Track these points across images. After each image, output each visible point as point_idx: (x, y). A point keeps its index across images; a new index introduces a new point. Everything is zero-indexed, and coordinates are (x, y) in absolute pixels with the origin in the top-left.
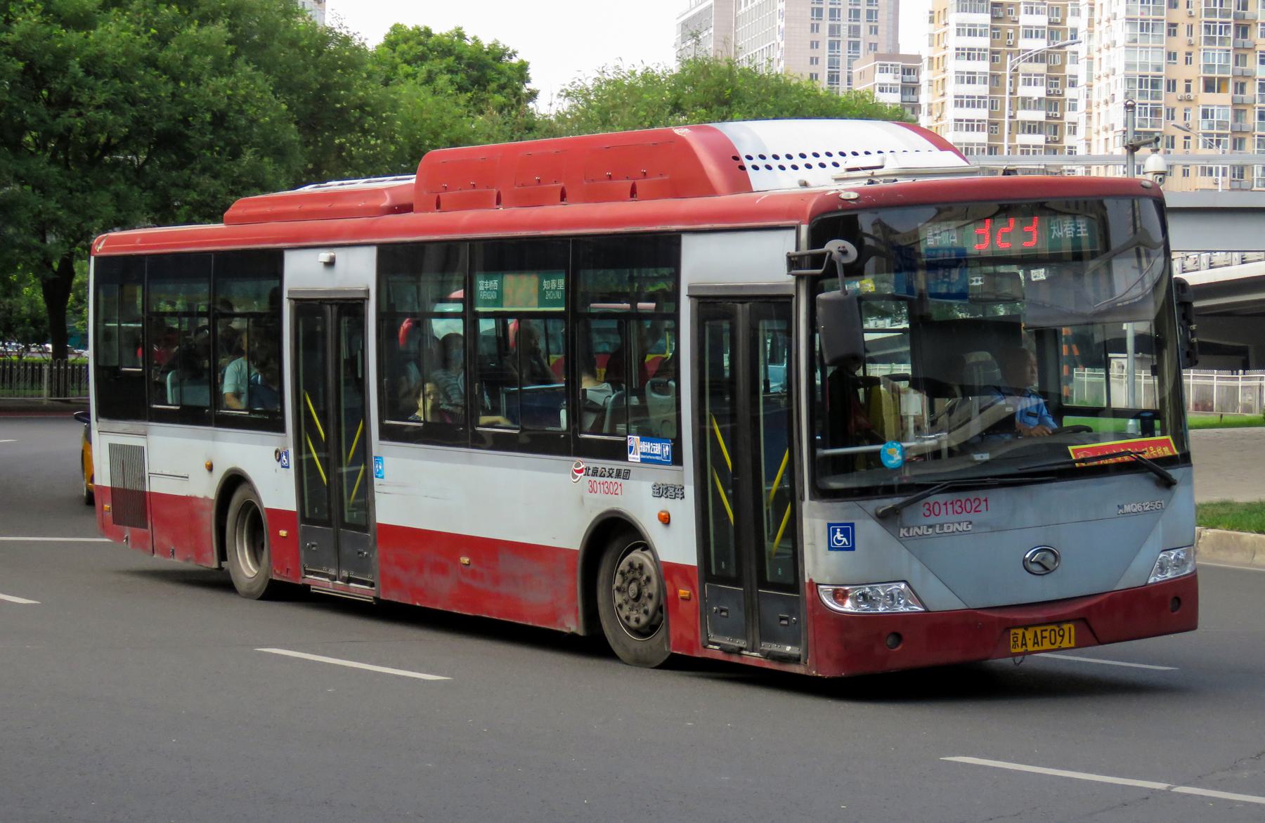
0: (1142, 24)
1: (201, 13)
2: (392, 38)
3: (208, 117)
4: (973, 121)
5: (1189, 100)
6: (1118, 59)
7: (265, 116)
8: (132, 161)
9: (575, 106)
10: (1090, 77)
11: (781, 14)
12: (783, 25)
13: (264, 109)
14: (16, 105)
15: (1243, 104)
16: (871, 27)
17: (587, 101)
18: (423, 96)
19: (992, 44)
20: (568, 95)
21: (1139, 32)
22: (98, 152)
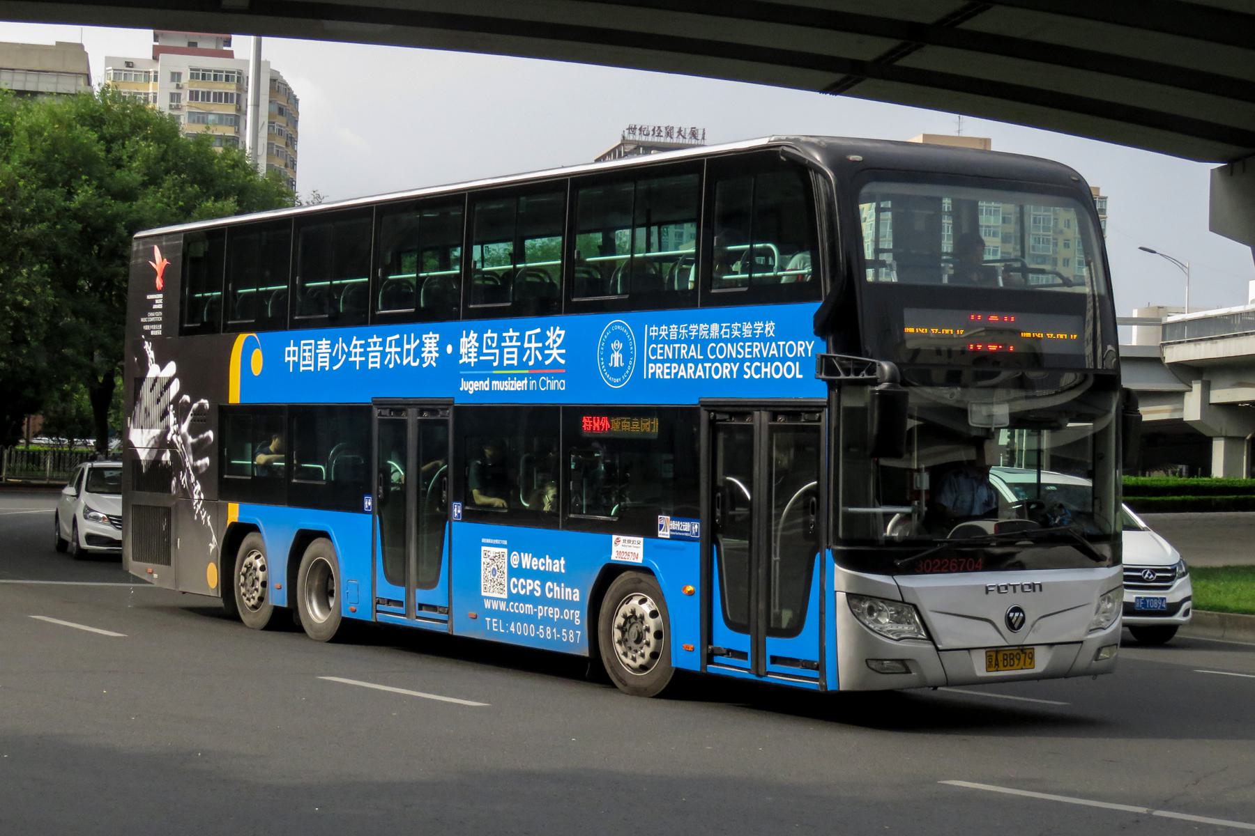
14: (75, 257)
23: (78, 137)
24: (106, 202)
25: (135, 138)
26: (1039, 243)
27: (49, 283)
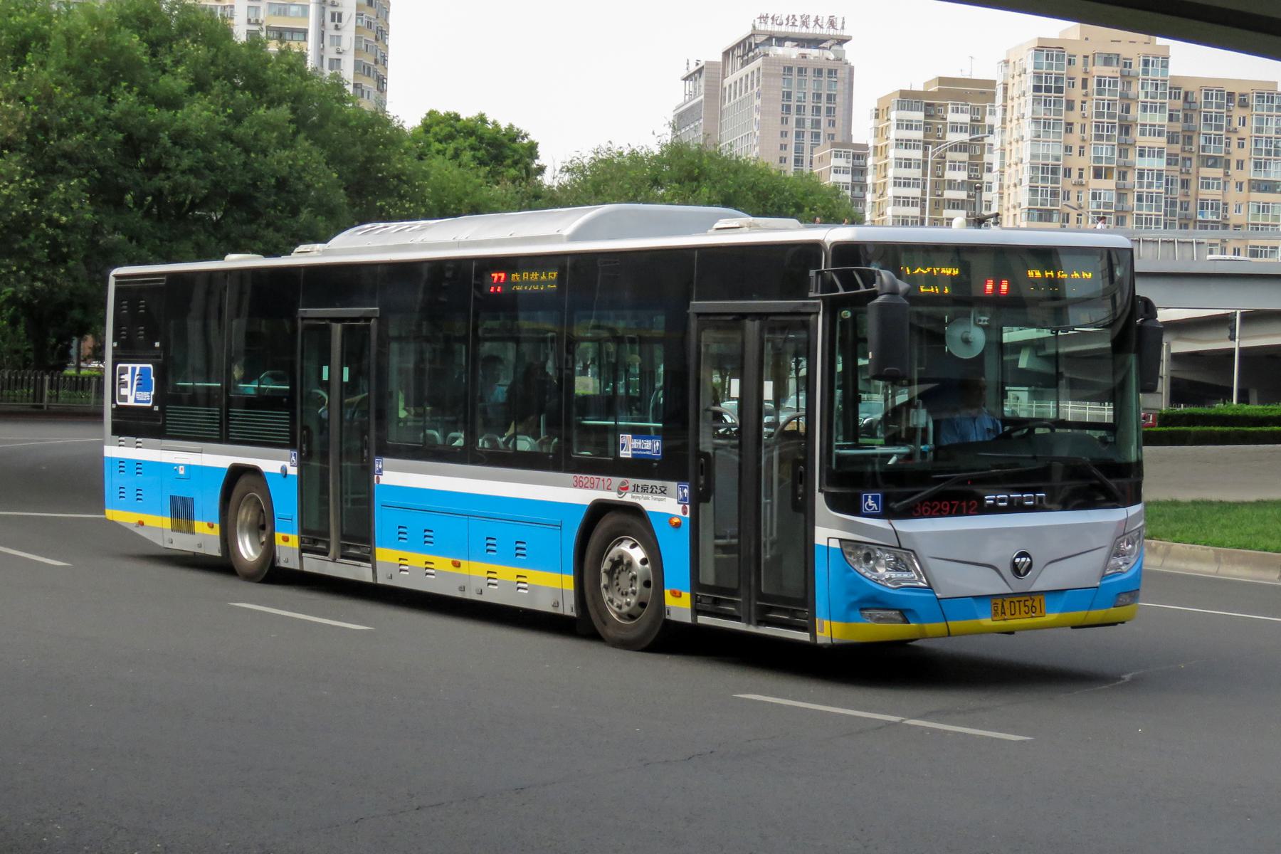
0: (1045, 123)
1: (269, 99)
2: (428, 122)
3: (273, 181)
4: (908, 198)
5: (1081, 185)
6: (1025, 150)
7: (318, 182)
8: (211, 218)
9: (574, 180)
10: (1002, 164)
11: (758, 109)
12: (758, 118)
13: (318, 177)
15: (1124, 188)
16: (830, 121)
17: (583, 175)
18: (450, 169)
19: (925, 137)
20: (568, 170)
21: (1042, 130)
22: (185, 209)
23: (119, 41)
24: (150, 110)
25: (182, 43)
26: (1210, 143)
27: (88, 199)
